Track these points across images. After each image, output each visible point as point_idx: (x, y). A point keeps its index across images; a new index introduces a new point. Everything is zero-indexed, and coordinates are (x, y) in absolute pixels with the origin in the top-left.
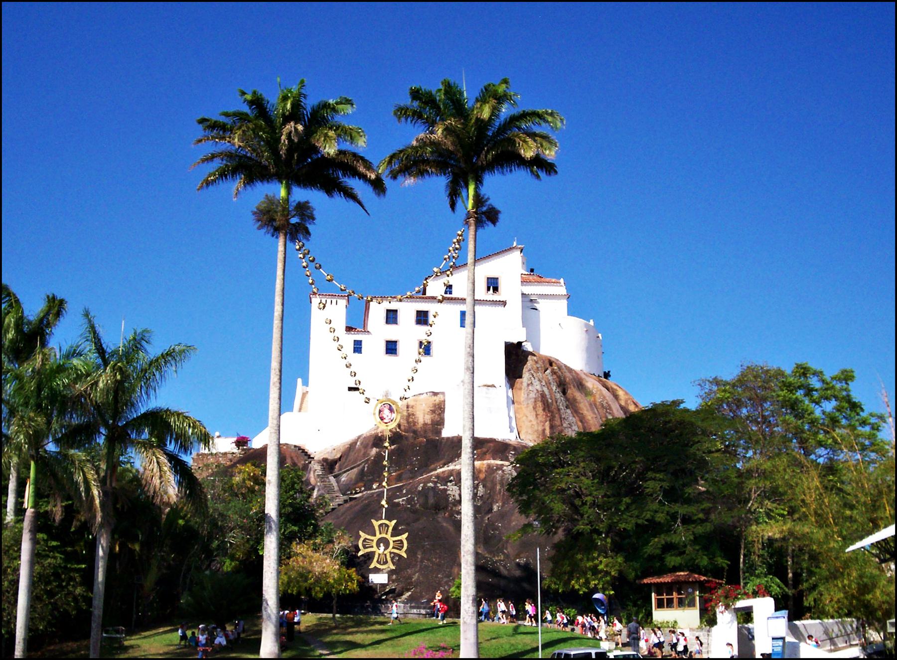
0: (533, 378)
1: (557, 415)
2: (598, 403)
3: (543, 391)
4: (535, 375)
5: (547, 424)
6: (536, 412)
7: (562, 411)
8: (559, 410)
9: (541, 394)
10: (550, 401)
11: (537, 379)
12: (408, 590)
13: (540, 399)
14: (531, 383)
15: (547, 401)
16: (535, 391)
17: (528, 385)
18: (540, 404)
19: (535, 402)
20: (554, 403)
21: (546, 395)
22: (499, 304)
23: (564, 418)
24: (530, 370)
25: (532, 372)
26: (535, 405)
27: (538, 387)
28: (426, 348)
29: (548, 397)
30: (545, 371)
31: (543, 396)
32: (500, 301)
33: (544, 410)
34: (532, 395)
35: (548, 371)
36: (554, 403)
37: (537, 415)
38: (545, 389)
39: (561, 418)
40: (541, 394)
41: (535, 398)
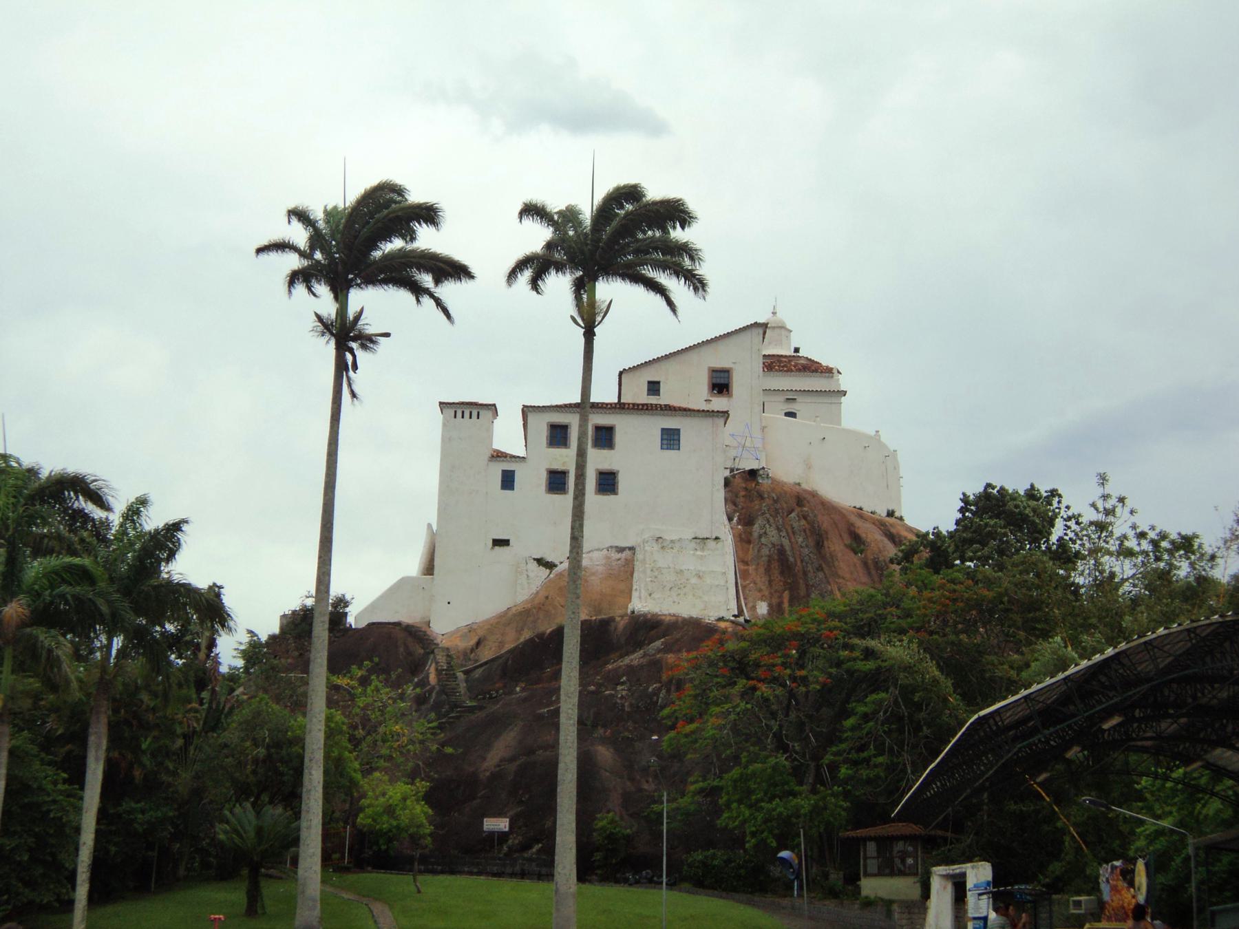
0: (767, 526)
1: (801, 581)
2: (870, 562)
3: (782, 546)
4: (771, 520)
5: (786, 595)
6: (770, 576)
7: (811, 575)
8: (805, 573)
9: (778, 550)
10: (791, 559)
11: (774, 526)
12: (538, 841)
13: (776, 557)
14: (765, 533)
15: (787, 560)
16: (770, 546)
17: (760, 536)
18: (775, 565)
19: (769, 561)
20: (799, 563)
21: (785, 551)
22: (717, 416)
23: (813, 586)
24: (763, 514)
25: (768, 515)
26: (769, 566)
27: (775, 540)
28: (608, 482)
29: (789, 553)
30: (788, 515)
31: (782, 551)
32: (718, 411)
33: (782, 573)
34: (765, 551)
35: (793, 515)
36: (799, 563)
37: (770, 582)
38: (786, 542)
39: (807, 585)
40: (778, 550)
41: (769, 556)
